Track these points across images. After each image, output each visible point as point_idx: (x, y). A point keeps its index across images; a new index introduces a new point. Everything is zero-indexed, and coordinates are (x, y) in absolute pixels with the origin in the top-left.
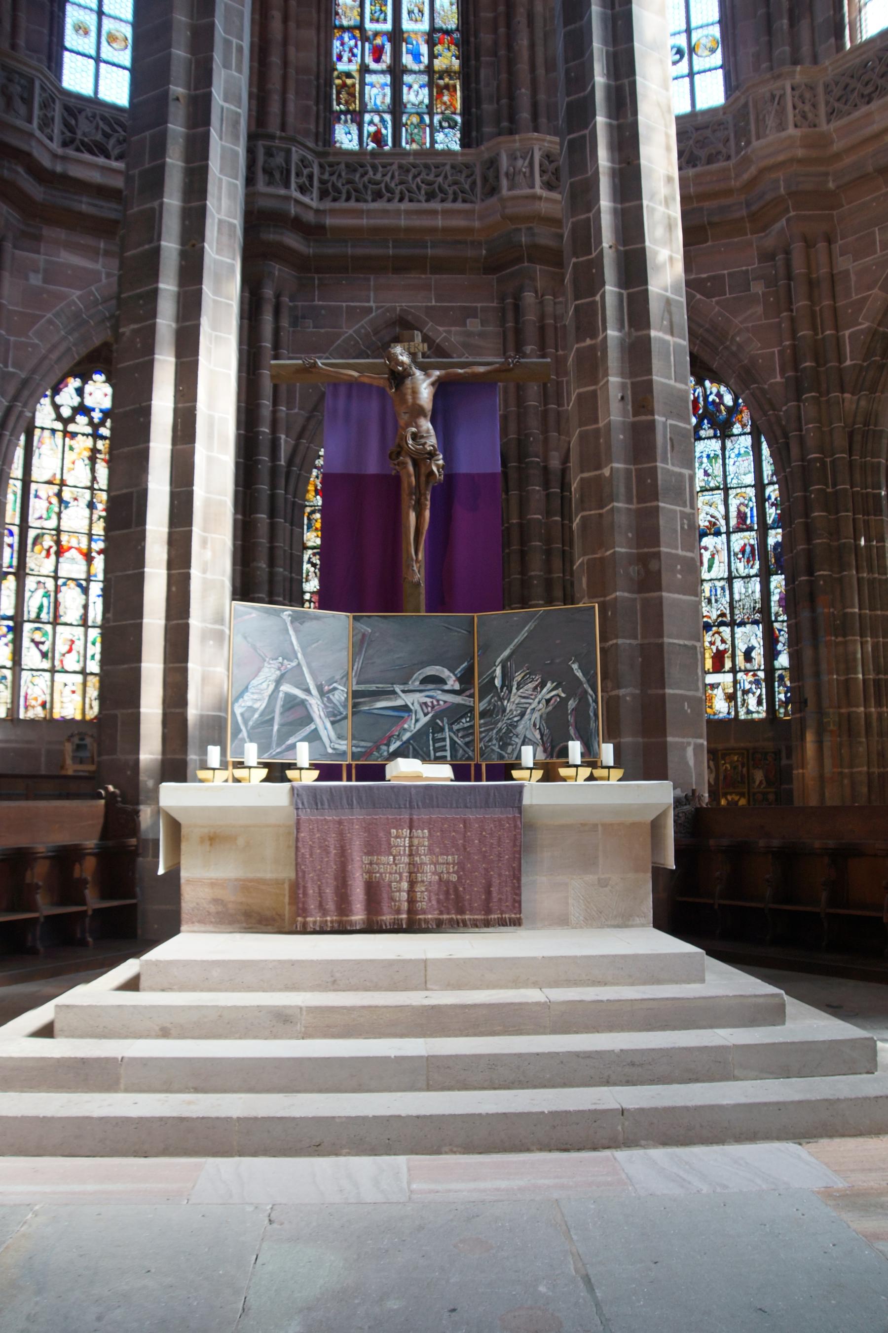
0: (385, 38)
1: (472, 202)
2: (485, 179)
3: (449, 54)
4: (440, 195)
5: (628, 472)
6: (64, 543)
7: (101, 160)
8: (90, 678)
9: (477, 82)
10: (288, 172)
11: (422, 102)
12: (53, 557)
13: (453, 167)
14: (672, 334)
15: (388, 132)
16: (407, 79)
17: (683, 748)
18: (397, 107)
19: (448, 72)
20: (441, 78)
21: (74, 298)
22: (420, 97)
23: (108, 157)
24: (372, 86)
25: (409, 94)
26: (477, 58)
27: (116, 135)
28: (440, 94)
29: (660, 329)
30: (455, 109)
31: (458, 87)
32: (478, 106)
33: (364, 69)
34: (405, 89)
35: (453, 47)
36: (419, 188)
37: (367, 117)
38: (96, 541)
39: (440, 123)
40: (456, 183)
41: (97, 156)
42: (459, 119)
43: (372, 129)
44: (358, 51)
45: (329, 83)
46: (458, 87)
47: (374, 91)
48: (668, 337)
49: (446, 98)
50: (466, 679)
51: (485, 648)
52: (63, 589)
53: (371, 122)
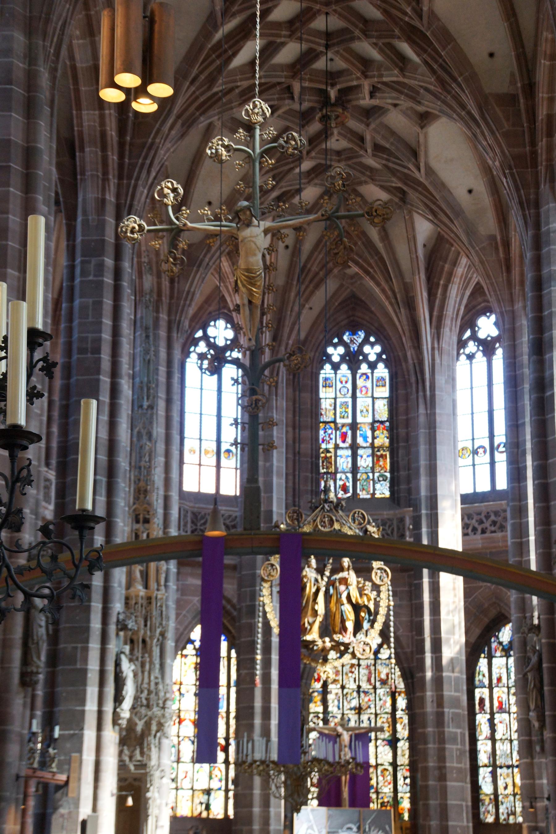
0: (348, 428)
2: (399, 529)
5: (434, 732)
6: (182, 717)
8: (196, 793)
9: (398, 457)
12: (177, 725)
15: (350, 484)
16: (360, 452)
18: (355, 469)
19: (380, 448)
20: (378, 451)
24: (341, 457)
26: (398, 442)
28: (378, 461)
29: (448, 671)
33: (337, 447)
34: (359, 458)
35: (385, 432)
37: (339, 476)
42: (388, 475)
43: (342, 483)
44: (333, 436)
45: (318, 457)
46: (388, 456)
47: (343, 460)
49: (381, 463)
50: (359, 828)
51: (364, 819)
52: (182, 743)
53: (341, 479)
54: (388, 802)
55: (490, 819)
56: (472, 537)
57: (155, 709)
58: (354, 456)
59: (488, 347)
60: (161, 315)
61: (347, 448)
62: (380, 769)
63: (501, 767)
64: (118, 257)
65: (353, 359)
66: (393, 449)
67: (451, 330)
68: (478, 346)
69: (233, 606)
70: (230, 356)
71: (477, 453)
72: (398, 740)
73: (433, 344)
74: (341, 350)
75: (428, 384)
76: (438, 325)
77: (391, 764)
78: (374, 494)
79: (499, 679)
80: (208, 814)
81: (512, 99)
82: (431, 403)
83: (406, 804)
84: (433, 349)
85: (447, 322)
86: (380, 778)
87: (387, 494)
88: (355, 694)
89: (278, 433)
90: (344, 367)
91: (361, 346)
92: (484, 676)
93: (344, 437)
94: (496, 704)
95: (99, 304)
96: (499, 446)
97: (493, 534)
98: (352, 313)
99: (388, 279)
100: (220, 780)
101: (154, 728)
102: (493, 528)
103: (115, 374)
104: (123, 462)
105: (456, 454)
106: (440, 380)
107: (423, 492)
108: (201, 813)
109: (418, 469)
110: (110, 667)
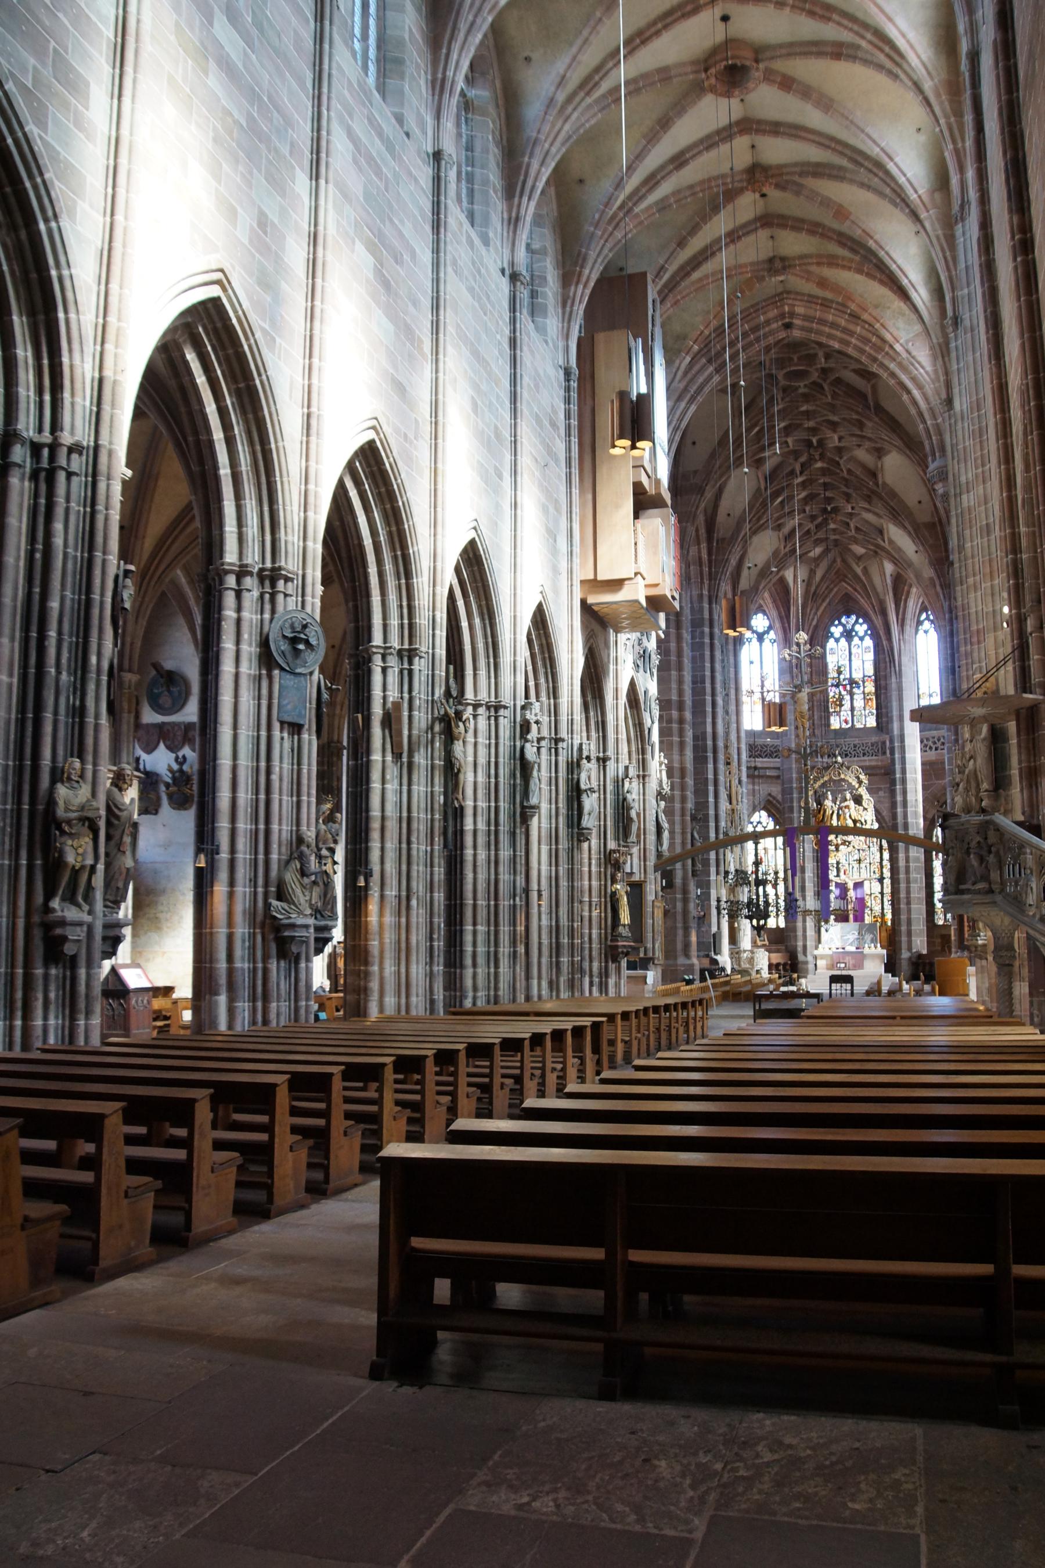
15: (849, 719)
18: (852, 709)
64: (711, 626)
65: (848, 635)
66: (877, 694)
74: (840, 629)
76: (902, 624)
81: (934, 524)
82: (900, 675)
85: (908, 622)
90: (843, 640)
95: (702, 656)
98: (848, 606)
99: (869, 597)
103: (713, 695)
104: (721, 744)
106: (905, 660)
107: (896, 732)
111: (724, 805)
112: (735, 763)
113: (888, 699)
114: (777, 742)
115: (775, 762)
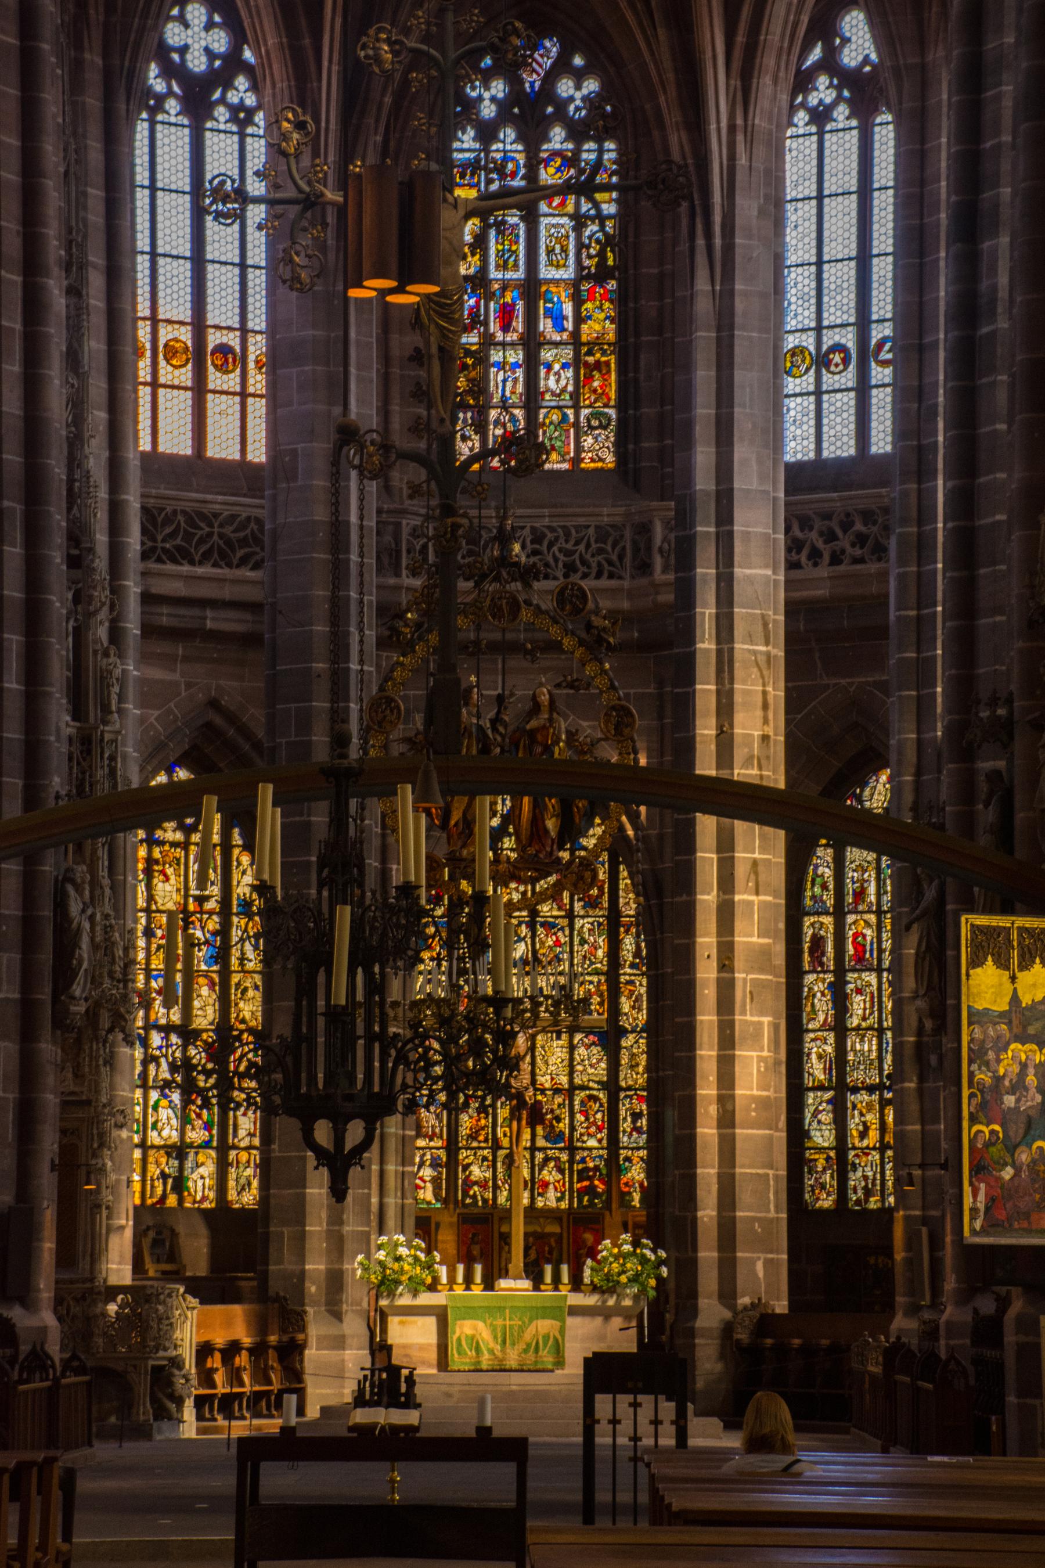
1: (620, 578)
2: (636, 550)
3: (602, 316)
4: (583, 569)
7: (186, 569)
8: (151, 1152)
9: (636, 370)
10: (398, 552)
11: (564, 390)
13: (597, 527)
14: (757, 893)
17: (753, 1262)
18: (532, 397)
20: (590, 353)
21: (152, 719)
22: (563, 382)
23: (192, 563)
25: (547, 379)
26: (637, 335)
27: (200, 533)
28: (590, 378)
30: (609, 399)
31: (613, 365)
32: (636, 408)
34: (543, 371)
35: (607, 305)
36: (556, 560)
38: (156, 978)
39: (589, 421)
40: (600, 551)
41: (181, 564)
42: (612, 412)
46: (613, 365)
48: (753, 898)
49: (596, 384)
54: (596, 1168)
55: (826, 1202)
56: (809, 572)
57: (107, 983)
58: (532, 365)
59: (863, 93)
60: (87, 56)
61: (513, 344)
62: (579, 1097)
63: (855, 1090)
65: (530, 114)
66: (626, 346)
67: (775, 80)
68: (839, 88)
69: (257, 746)
70: (222, 100)
71: (827, 364)
72: (623, 1032)
73: (732, 116)
75: (717, 219)
77: (603, 1086)
78: (577, 460)
79: (860, 895)
80: (181, 1201)
82: (726, 269)
83: (636, 1173)
84: (732, 128)
86: (580, 1118)
87: (610, 460)
88: (524, 930)
89: (358, 333)
90: (509, 133)
91: (551, 78)
92: (824, 887)
93: (506, 315)
94: (851, 950)
96: (880, 345)
97: (859, 567)
100: (208, 1127)
101: (105, 1022)
102: (858, 552)
105: (779, 364)
107: (704, 481)
108: (164, 1197)
109: (689, 425)
110: (47, 912)
111: (60, 721)
112: (101, 563)
113: (676, 360)
114: (246, 506)
115: (244, 581)
